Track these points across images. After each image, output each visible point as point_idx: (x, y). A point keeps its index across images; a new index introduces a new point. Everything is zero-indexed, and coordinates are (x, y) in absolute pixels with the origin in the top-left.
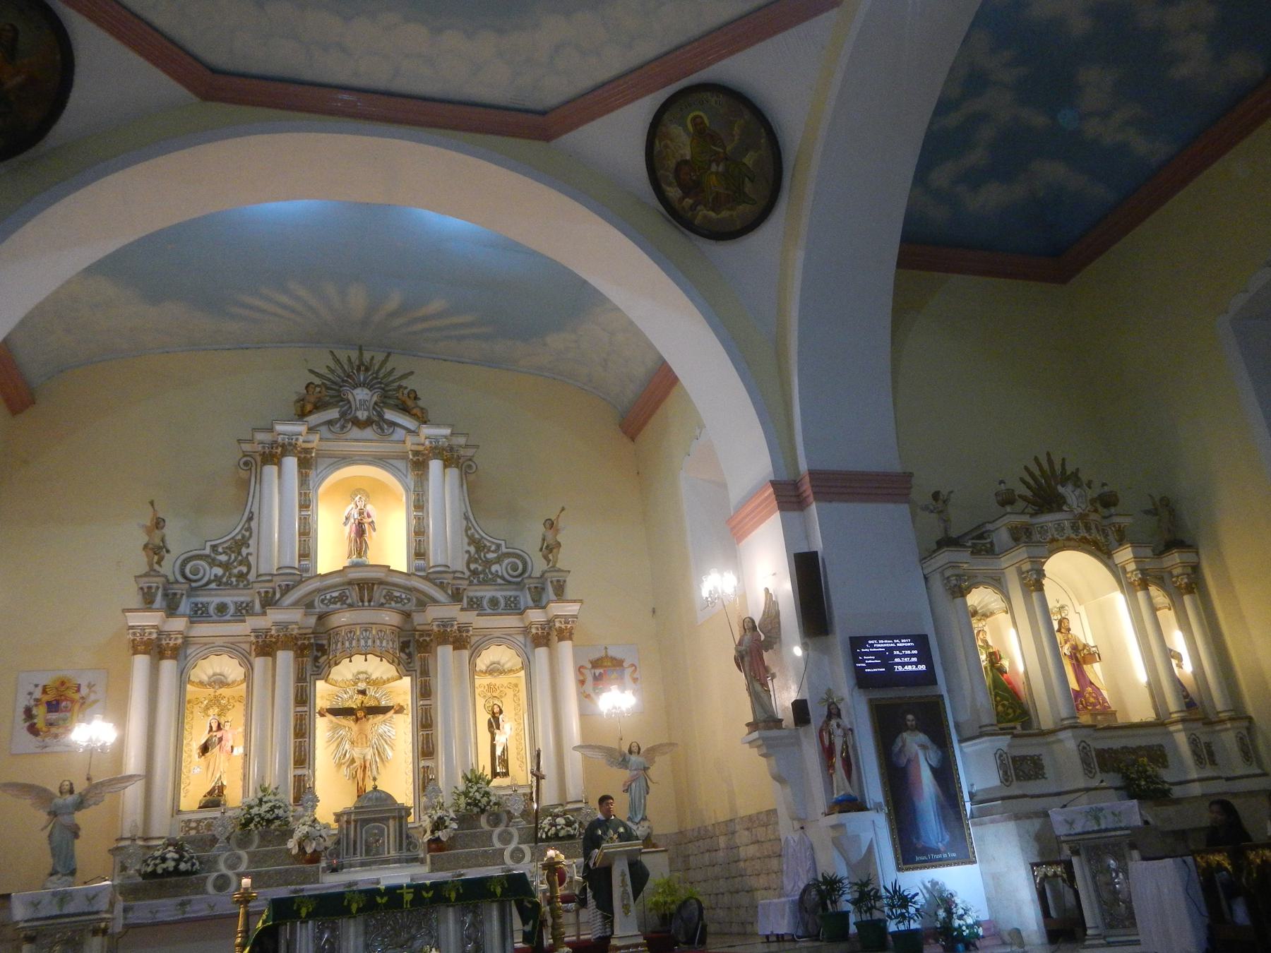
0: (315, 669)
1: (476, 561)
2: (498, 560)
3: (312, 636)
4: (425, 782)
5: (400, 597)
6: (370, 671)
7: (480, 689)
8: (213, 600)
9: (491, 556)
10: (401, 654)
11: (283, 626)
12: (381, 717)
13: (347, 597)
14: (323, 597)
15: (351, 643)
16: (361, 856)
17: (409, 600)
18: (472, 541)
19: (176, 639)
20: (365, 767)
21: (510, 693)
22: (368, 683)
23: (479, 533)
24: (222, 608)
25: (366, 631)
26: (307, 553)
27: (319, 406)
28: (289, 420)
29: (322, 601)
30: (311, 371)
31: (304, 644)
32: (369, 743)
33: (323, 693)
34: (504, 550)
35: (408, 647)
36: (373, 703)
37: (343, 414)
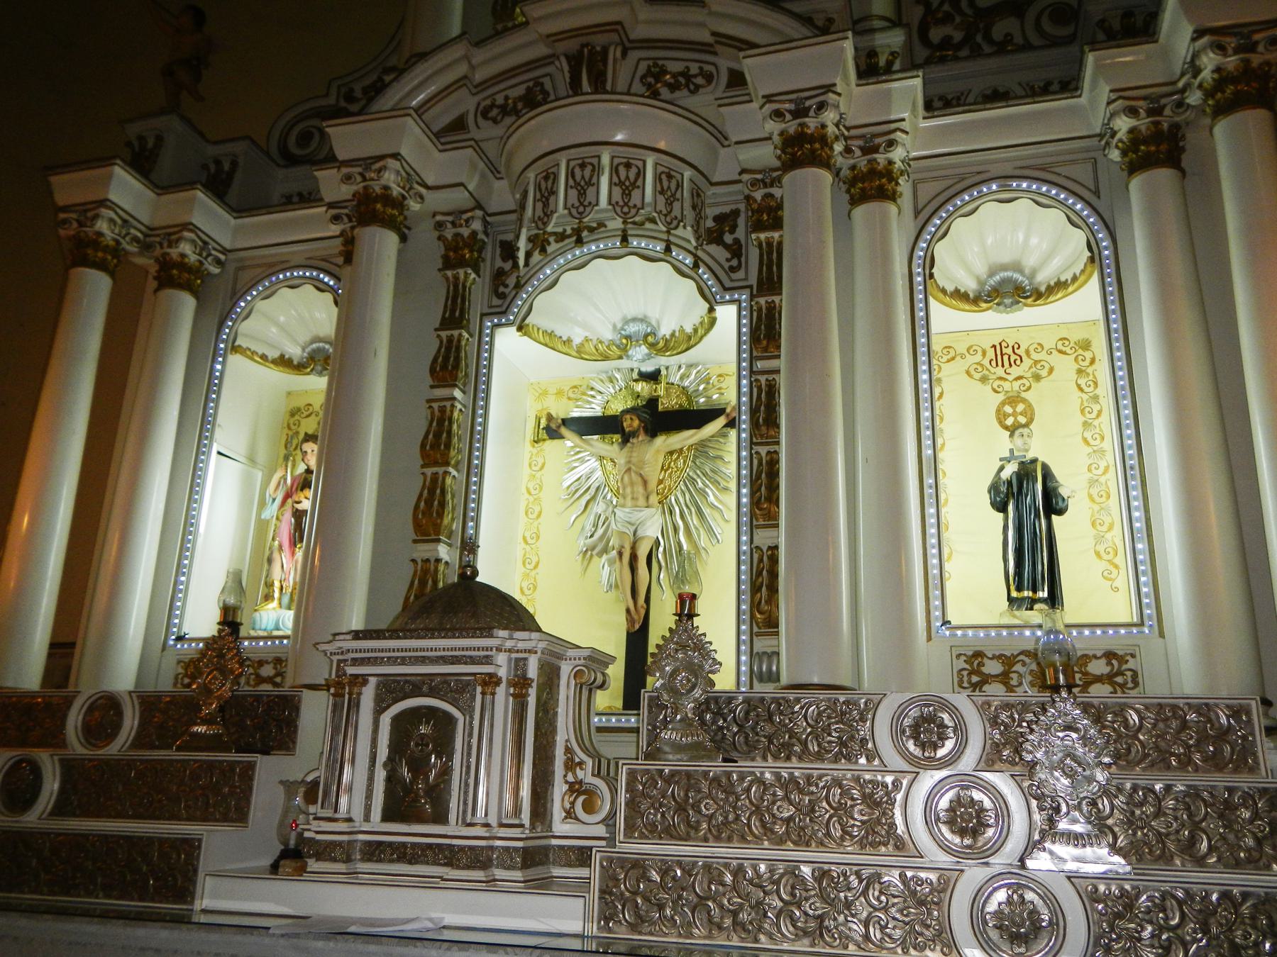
0: (496, 301)
1: (947, 19)
3: (479, 213)
5: (686, 74)
6: (653, 315)
7: (971, 360)
10: (713, 249)
13: (546, 93)
14: (488, 102)
15: (546, 205)
16: (367, 818)
17: (709, 78)
19: (178, 241)
20: (634, 558)
21: (1065, 366)
22: (652, 346)
25: (583, 166)
29: (485, 114)
31: (457, 235)
32: (654, 499)
35: (732, 231)
36: (668, 402)
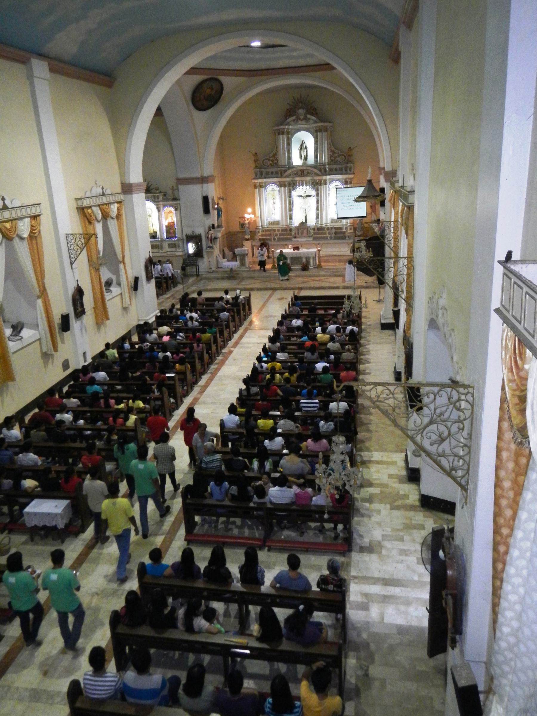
2: (339, 156)
4: (318, 217)
8: (271, 170)
9: (336, 155)
11: (284, 182)
12: (309, 198)
18: (332, 151)
23: (333, 149)
24: (272, 173)
26: (290, 158)
27: (290, 116)
28: (282, 124)
30: (288, 104)
33: (295, 193)
34: (340, 153)
36: (307, 194)
37: (297, 118)
